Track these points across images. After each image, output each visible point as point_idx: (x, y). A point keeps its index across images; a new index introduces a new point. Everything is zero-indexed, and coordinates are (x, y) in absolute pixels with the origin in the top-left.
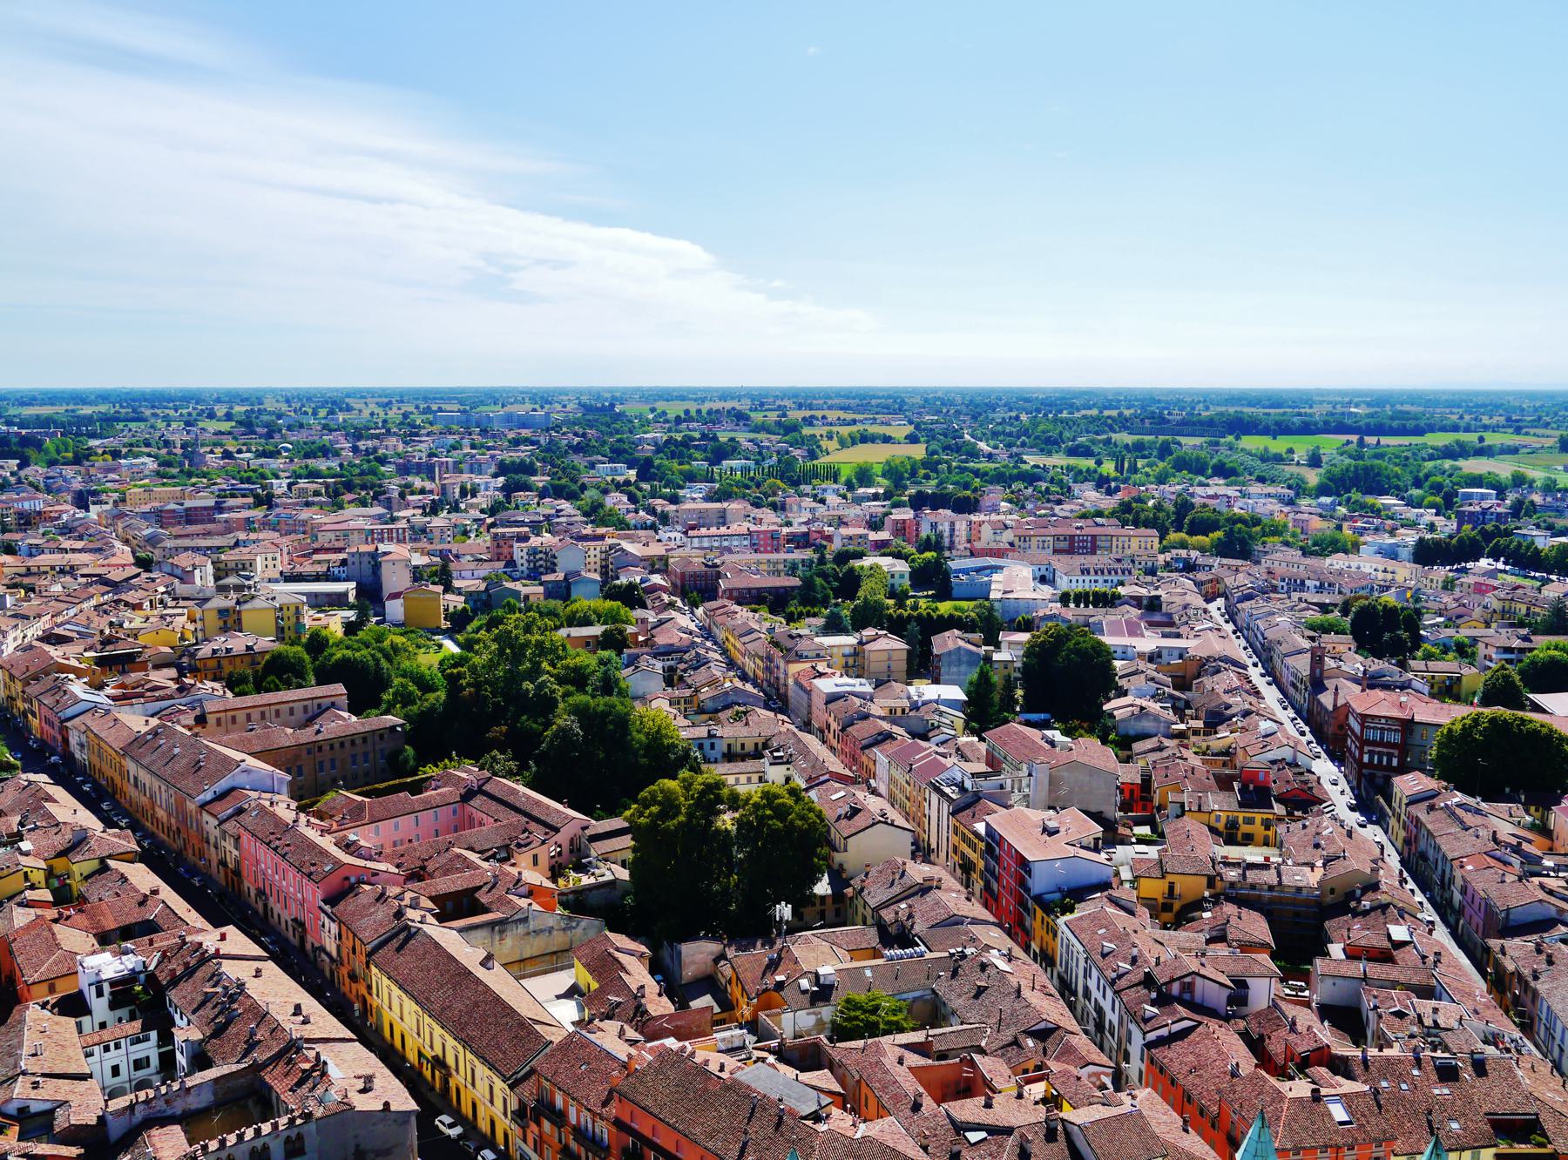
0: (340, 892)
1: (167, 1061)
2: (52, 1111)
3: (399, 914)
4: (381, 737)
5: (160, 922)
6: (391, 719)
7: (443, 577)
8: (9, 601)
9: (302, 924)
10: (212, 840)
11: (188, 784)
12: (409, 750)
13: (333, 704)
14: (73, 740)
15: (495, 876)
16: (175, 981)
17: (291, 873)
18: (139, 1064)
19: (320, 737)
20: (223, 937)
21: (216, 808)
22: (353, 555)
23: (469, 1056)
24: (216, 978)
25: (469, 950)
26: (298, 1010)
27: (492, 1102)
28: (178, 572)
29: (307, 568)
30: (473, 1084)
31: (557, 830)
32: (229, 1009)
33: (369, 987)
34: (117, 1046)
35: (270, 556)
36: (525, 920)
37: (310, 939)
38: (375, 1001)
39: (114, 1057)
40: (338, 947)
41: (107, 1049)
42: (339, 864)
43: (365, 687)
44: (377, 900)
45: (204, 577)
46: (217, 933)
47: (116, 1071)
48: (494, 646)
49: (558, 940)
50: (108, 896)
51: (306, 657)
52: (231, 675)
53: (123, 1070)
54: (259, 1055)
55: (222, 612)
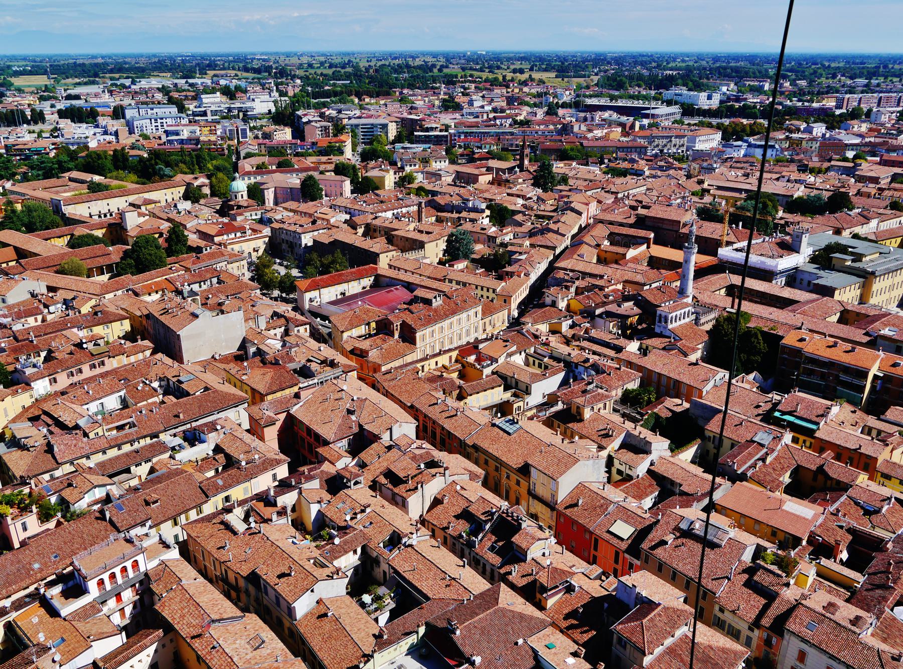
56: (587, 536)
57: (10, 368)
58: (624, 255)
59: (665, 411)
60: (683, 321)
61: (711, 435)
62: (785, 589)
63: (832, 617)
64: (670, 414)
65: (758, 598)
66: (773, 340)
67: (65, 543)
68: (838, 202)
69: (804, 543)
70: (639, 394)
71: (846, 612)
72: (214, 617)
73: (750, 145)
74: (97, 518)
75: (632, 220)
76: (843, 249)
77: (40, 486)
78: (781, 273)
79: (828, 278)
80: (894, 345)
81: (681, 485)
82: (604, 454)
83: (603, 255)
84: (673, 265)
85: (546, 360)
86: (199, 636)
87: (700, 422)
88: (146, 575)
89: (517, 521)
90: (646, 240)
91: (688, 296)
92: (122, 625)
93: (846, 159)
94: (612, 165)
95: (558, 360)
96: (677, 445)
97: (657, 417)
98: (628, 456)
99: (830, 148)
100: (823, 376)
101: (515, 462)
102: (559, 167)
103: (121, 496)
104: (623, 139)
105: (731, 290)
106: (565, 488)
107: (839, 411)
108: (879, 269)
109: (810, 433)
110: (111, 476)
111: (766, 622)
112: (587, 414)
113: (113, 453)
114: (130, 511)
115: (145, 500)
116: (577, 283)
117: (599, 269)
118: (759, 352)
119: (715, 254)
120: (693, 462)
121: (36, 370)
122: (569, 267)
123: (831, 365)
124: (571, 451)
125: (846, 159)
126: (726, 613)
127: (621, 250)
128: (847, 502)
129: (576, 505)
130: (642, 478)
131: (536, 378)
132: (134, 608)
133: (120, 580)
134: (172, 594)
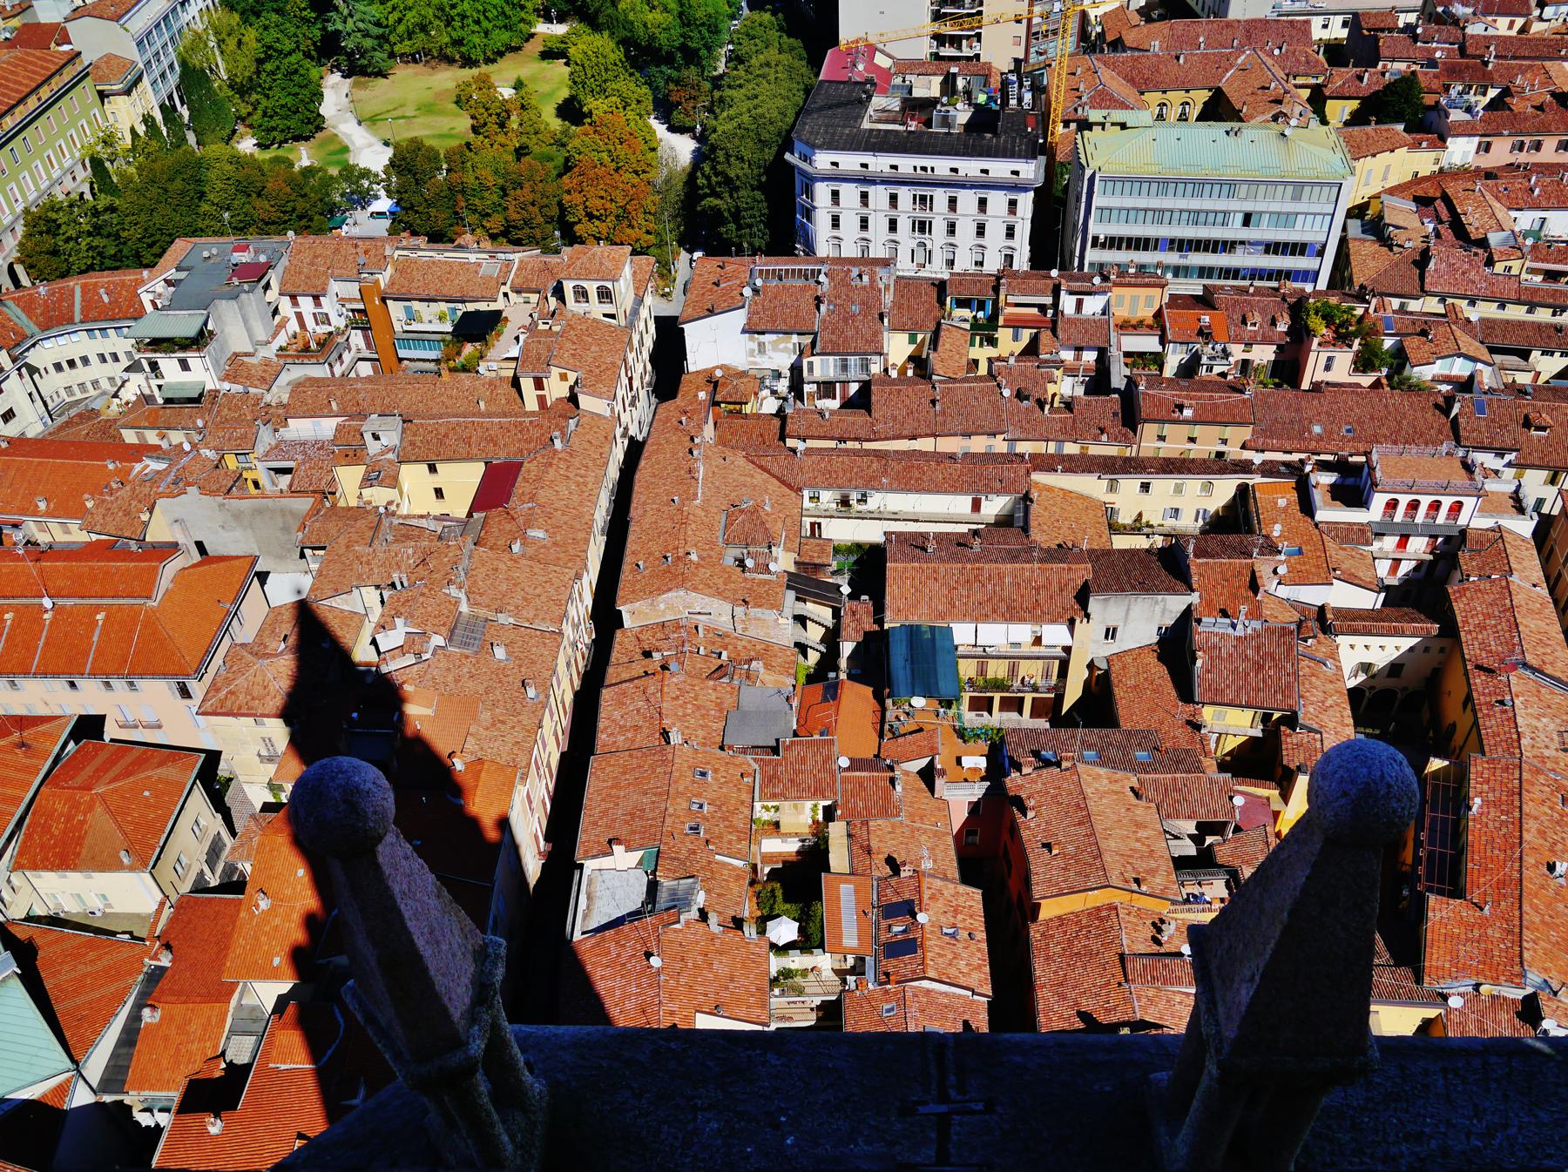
57: (1429, 100)
67: (1372, 418)
72: (1529, 658)
74: (1437, 406)
77: (1380, 314)
86: (1490, 671)
88: (1463, 532)
92: (1387, 582)
103: (1491, 391)
110: (1493, 350)
113: (1516, 313)
114: (1493, 421)
115: (1526, 417)
121: (1467, 117)
132: (1416, 569)
133: (1420, 517)
134: (1485, 585)
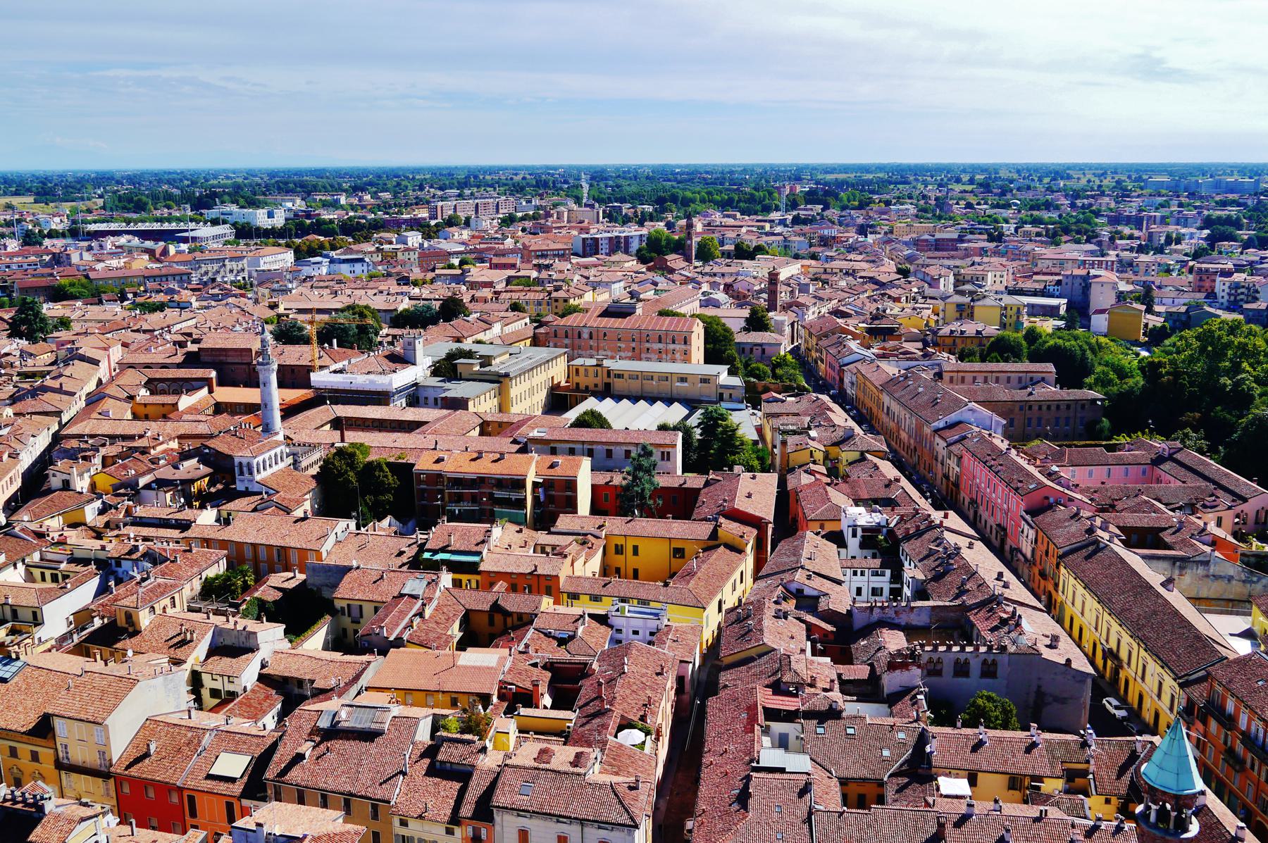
0: (1040, 508)
1: (896, 593)
2: (817, 598)
3: (1090, 531)
4: (1083, 407)
5: (899, 501)
6: (1093, 394)
7: (1147, 298)
8: (812, 289)
9: (1004, 529)
10: (940, 458)
11: (927, 413)
12: (1106, 422)
13: (1043, 379)
14: (846, 380)
15: (1180, 522)
16: (908, 537)
17: (1001, 488)
18: (876, 592)
19: (1031, 398)
20: (946, 516)
21: (947, 433)
22: (1067, 276)
23: (1143, 653)
24: (939, 540)
25: (1150, 572)
26: (1000, 575)
27: (1159, 696)
28: (928, 279)
29: (1028, 285)
30: (1143, 678)
31: (1245, 500)
32: (946, 564)
33: (1056, 585)
34: (862, 574)
35: (998, 274)
36: (1206, 563)
37: (1009, 542)
38: (1060, 597)
39: (859, 581)
40: (1033, 550)
41: (855, 574)
42: (1040, 483)
43: (1072, 369)
44: (1072, 518)
45: (947, 284)
46: (942, 513)
47: (859, 591)
48: (1196, 344)
49: (1236, 590)
50: (864, 476)
51: (1024, 343)
52: (963, 350)
53: (864, 592)
54: (970, 600)
55: (960, 307)
56: (175, 799)
58: (175, 405)
59: (272, 591)
60: (275, 468)
61: (344, 604)
62: (482, 756)
63: (547, 766)
64: (280, 594)
65: (450, 784)
66: (403, 470)
68: (451, 310)
69: (495, 699)
70: (228, 579)
71: (563, 755)
73: (332, 261)
75: (179, 358)
76: (469, 354)
78: (399, 391)
79: (456, 390)
80: (547, 448)
81: (312, 682)
82: (184, 673)
83: (142, 411)
84: (250, 408)
85: (63, 566)
87: (326, 594)
89: (35, 805)
90: (207, 382)
91: (277, 434)
93: (451, 267)
94: (139, 300)
95: (85, 562)
96: (296, 630)
97: (262, 604)
98: (224, 664)
99: (429, 259)
100: (474, 499)
101: (24, 720)
102: (51, 310)
104: (155, 266)
105: (337, 424)
106: (120, 736)
107: (501, 533)
108: (513, 371)
109: (472, 568)
111: (467, 810)
112: (145, 619)
116: (103, 451)
117: (137, 427)
118: (388, 490)
119: (306, 384)
120: (325, 648)
122: (87, 431)
123: (481, 481)
124: (123, 673)
125: (451, 267)
126: (411, 823)
127: (169, 399)
128: (536, 636)
129: (147, 755)
130: (253, 691)
131: (48, 596)
